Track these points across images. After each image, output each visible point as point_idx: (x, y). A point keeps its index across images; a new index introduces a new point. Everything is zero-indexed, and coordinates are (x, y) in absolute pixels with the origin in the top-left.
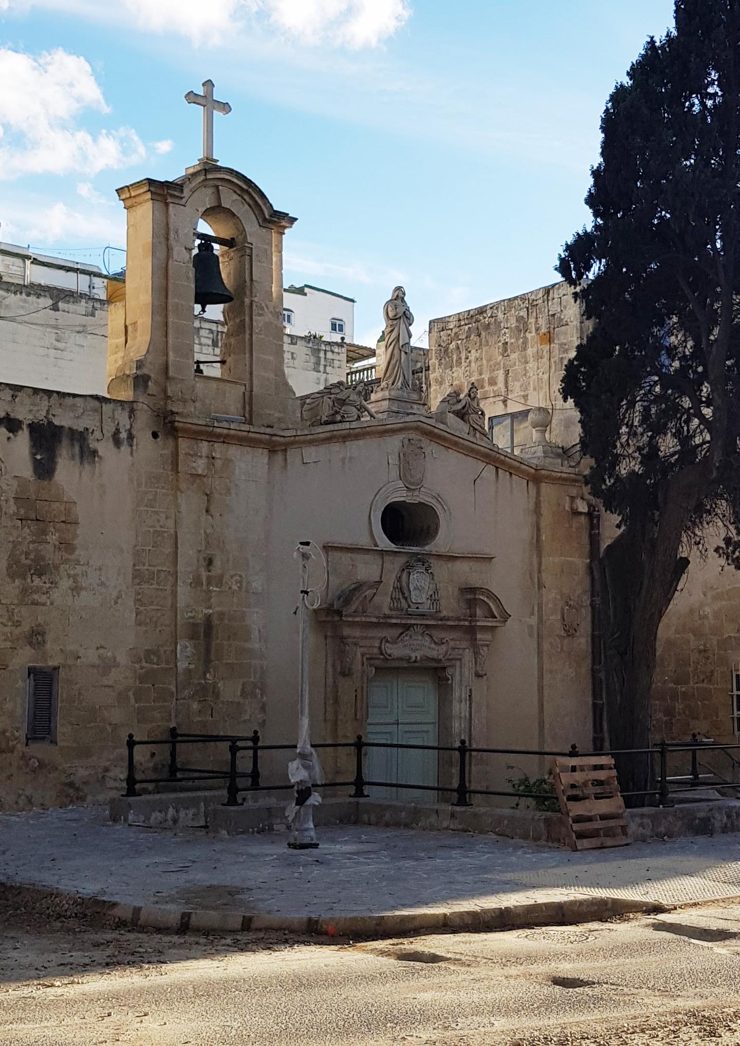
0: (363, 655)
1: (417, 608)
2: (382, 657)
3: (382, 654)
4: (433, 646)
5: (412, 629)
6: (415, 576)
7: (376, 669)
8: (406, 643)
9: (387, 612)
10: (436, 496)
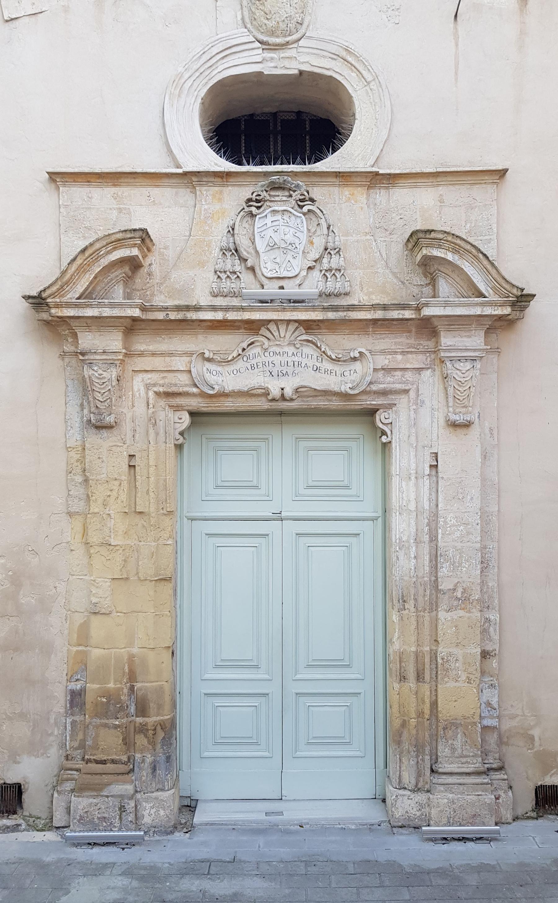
0: (148, 387)
1: (282, 288)
2: (195, 390)
3: (195, 386)
4: (327, 365)
5: (263, 331)
6: (270, 218)
7: (192, 414)
8: (254, 362)
9: (205, 300)
10: (344, 54)
